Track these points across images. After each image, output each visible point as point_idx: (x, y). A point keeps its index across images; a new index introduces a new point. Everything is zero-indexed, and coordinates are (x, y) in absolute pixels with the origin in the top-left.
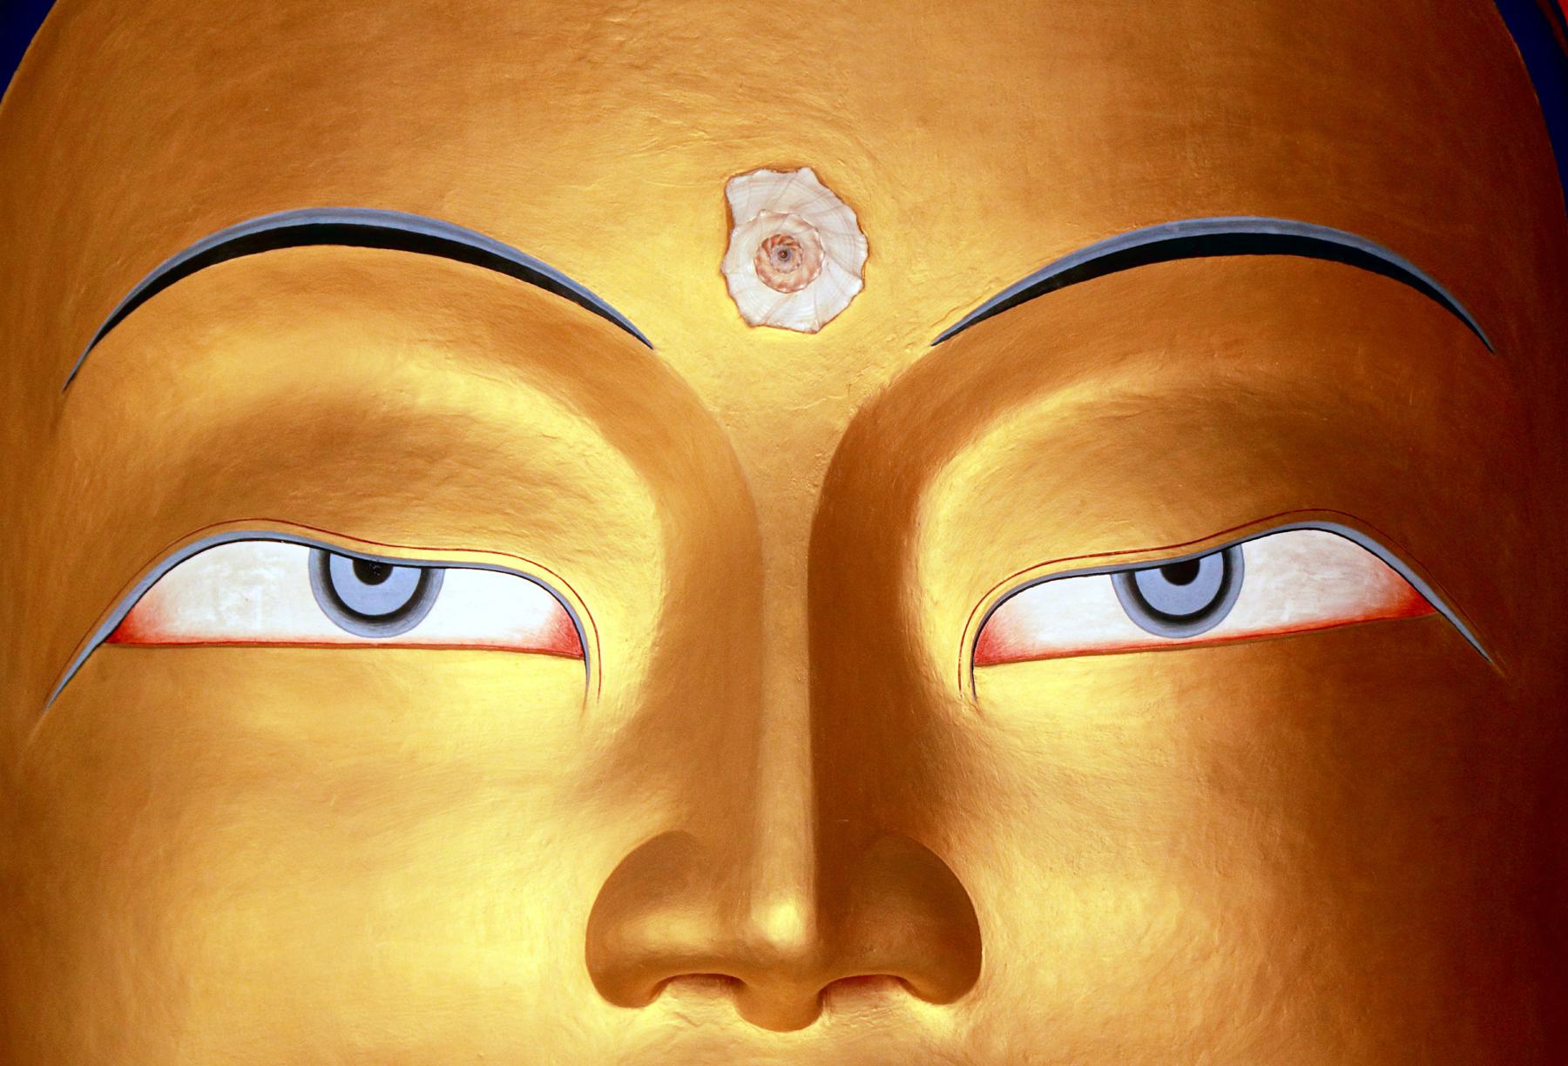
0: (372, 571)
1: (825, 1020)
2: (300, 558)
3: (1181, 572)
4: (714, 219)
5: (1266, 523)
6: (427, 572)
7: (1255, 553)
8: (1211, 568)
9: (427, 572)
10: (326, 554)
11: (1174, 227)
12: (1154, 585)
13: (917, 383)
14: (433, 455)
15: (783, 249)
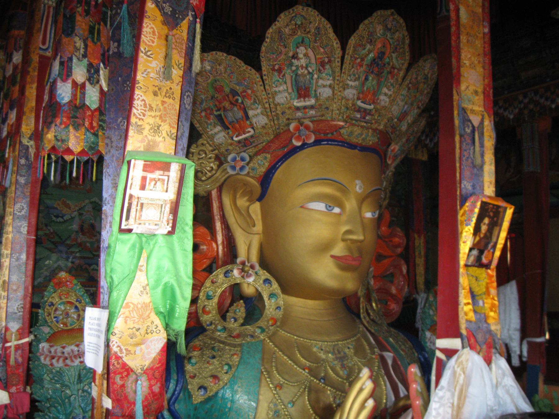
0: (330, 207)
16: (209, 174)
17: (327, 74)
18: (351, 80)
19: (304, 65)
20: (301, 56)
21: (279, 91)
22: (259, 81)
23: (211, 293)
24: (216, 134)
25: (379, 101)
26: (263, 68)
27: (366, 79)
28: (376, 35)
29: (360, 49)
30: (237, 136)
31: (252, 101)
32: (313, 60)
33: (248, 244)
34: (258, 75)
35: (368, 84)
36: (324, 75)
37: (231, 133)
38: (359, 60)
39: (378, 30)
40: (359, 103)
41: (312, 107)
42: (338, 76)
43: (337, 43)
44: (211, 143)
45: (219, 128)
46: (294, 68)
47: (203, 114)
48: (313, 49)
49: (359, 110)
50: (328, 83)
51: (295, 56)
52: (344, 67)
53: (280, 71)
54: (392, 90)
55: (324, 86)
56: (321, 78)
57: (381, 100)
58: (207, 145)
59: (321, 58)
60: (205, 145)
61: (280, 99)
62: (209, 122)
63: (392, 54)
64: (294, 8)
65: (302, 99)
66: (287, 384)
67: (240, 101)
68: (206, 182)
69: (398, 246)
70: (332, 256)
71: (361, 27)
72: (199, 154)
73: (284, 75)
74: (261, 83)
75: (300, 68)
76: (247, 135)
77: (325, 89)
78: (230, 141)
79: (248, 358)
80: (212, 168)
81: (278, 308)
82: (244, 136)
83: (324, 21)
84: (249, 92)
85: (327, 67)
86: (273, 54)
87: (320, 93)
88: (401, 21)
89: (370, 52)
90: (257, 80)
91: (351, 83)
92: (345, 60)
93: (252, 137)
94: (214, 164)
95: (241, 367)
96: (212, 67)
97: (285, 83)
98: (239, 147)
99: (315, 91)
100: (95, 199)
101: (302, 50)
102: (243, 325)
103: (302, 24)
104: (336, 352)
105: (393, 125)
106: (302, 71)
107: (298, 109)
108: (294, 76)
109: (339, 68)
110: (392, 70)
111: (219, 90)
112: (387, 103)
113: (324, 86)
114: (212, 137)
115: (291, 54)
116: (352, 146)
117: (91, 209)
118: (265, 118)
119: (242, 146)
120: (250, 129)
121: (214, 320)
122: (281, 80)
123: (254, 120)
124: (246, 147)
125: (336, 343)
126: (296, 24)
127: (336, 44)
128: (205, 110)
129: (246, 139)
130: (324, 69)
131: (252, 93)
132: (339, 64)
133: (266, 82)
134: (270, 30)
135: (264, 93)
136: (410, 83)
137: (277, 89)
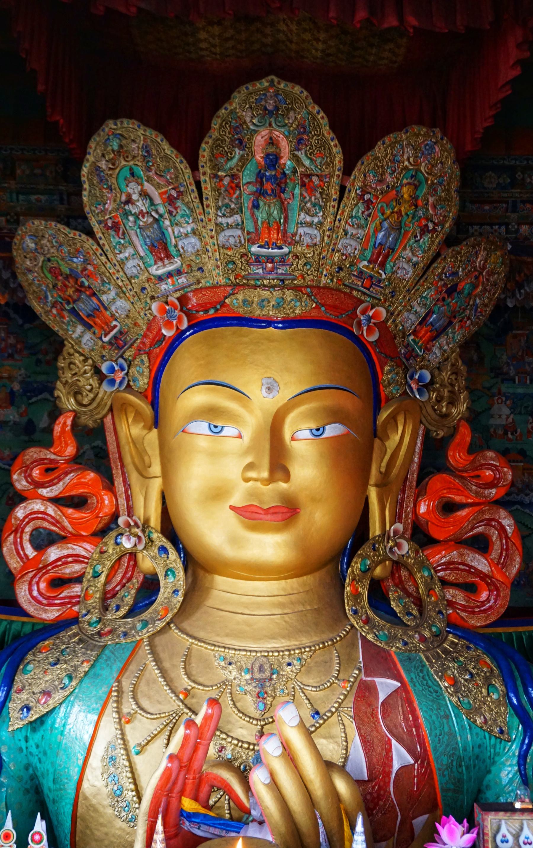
0: (216, 427)
1: (270, 485)
2: (207, 424)
3: (318, 430)
4: (260, 384)
5: (328, 424)
6: (223, 427)
7: (327, 427)
8: (321, 429)
9: (223, 427)
10: (210, 424)
11: (319, 385)
12: (314, 431)
13: (285, 405)
14: (223, 412)
15: (269, 389)
16: (91, 396)
17: (183, 216)
18: (224, 216)
19: (145, 211)
20: (135, 197)
21: (127, 259)
22: (97, 250)
23: (99, 568)
24: (81, 337)
25: (297, 238)
26: (95, 230)
27: (256, 206)
28: (248, 127)
29: (222, 160)
30: (105, 336)
31: (99, 281)
32: (158, 200)
33: (144, 494)
34: (91, 241)
35: (261, 215)
36: (178, 218)
37: (96, 331)
38: (227, 181)
39: (248, 119)
40: (255, 249)
41: (179, 272)
42: (200, 214)
43: (181, 162)
44: (81, 350)
45: (80, 329)
46: (131, 218)
47: (54, 311)
48: (149, 180)
49: (258, 260)
50: (189, 229)
51: (129, 201)
52: (204, 196)
53: (116, 227)
54: (321, 214)
55: (187, 235)
56: (177, 224)
57: (301, 236)
58: (77, 355)
59: (166, 192)
60: (73, 355)
61: (131, 267)
62: (65, 321)
63: (298, 153)
64: (104, 126)
65: (160, 264)
66: (140, 714)
67: (86, 284)
68: (91, 407)
69: (491, 485)
70: (232, 508)
71: (216, 124)
72: (71, 369)
73: (124, 234)
74: (100, 251)
75: (140, 217)
76: (115, 331)
77: (189, 239)
78: (100, 343)
79: (102, 669)
80: (91, 385)
81: (176, 592)
82: (112, 333)
83: (151, 133)
84: (90, 267)
85: (179, 203)
86: (99, 205)
87: (183, 248)
88: (297, 89)
89: (244, 161)
90: (94, 248)
91: (224, 221)
92: (203, 186)
93: (121, 332)
94: (93, 380)
95: (86, 681)
96: (36, 244)
97: (131, 243)
98: (113, 351)
99: (176, 246)
100: (98, 443)
101: (133, 189)
102: (125, 617)
103: (121, 146)
104: (256, 669)
105: (361, 272)
106: (145, 220)
107: (160, 279)
108: (138, 230)
109: (198, 200)
110: (307, 181)
111: (56, 272)
112: (318, 239)
113: (187, 235)
114: (78, 341)
115: (124, 198)
116: (269, 323)
117: (92, 457)
118: (124, 302)
119: (116, 349)
120: (114, 323)
121: (94, 608)
122: (122, 241)
123: (113, 308)
124: (121, 349)
125: (266, 654)
126: (113, 151)
127: (183, 167)
128: (54, 305)
129: (115, 337)
130: (176, 209)
131: (94, 268)
132: (196, 194)
133: (107, 247)
134: (85, 171)
135: (108, 265)
136: (364, 192)
137: (121, 256)
